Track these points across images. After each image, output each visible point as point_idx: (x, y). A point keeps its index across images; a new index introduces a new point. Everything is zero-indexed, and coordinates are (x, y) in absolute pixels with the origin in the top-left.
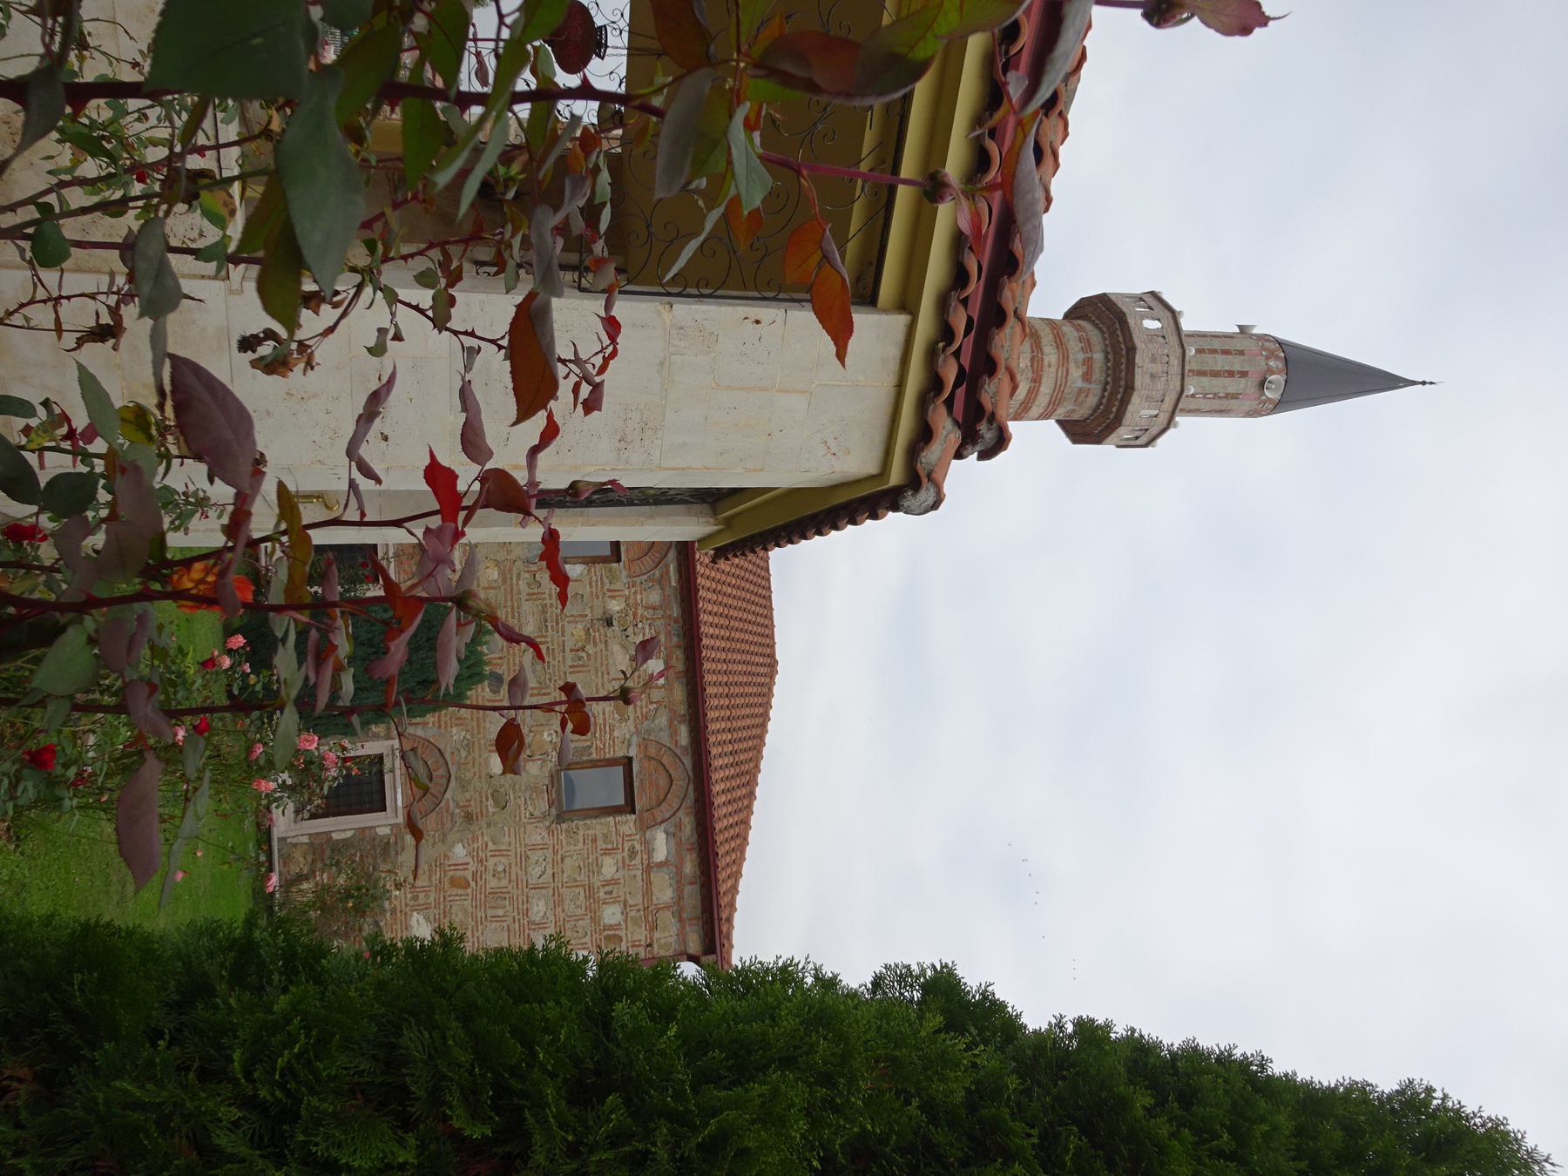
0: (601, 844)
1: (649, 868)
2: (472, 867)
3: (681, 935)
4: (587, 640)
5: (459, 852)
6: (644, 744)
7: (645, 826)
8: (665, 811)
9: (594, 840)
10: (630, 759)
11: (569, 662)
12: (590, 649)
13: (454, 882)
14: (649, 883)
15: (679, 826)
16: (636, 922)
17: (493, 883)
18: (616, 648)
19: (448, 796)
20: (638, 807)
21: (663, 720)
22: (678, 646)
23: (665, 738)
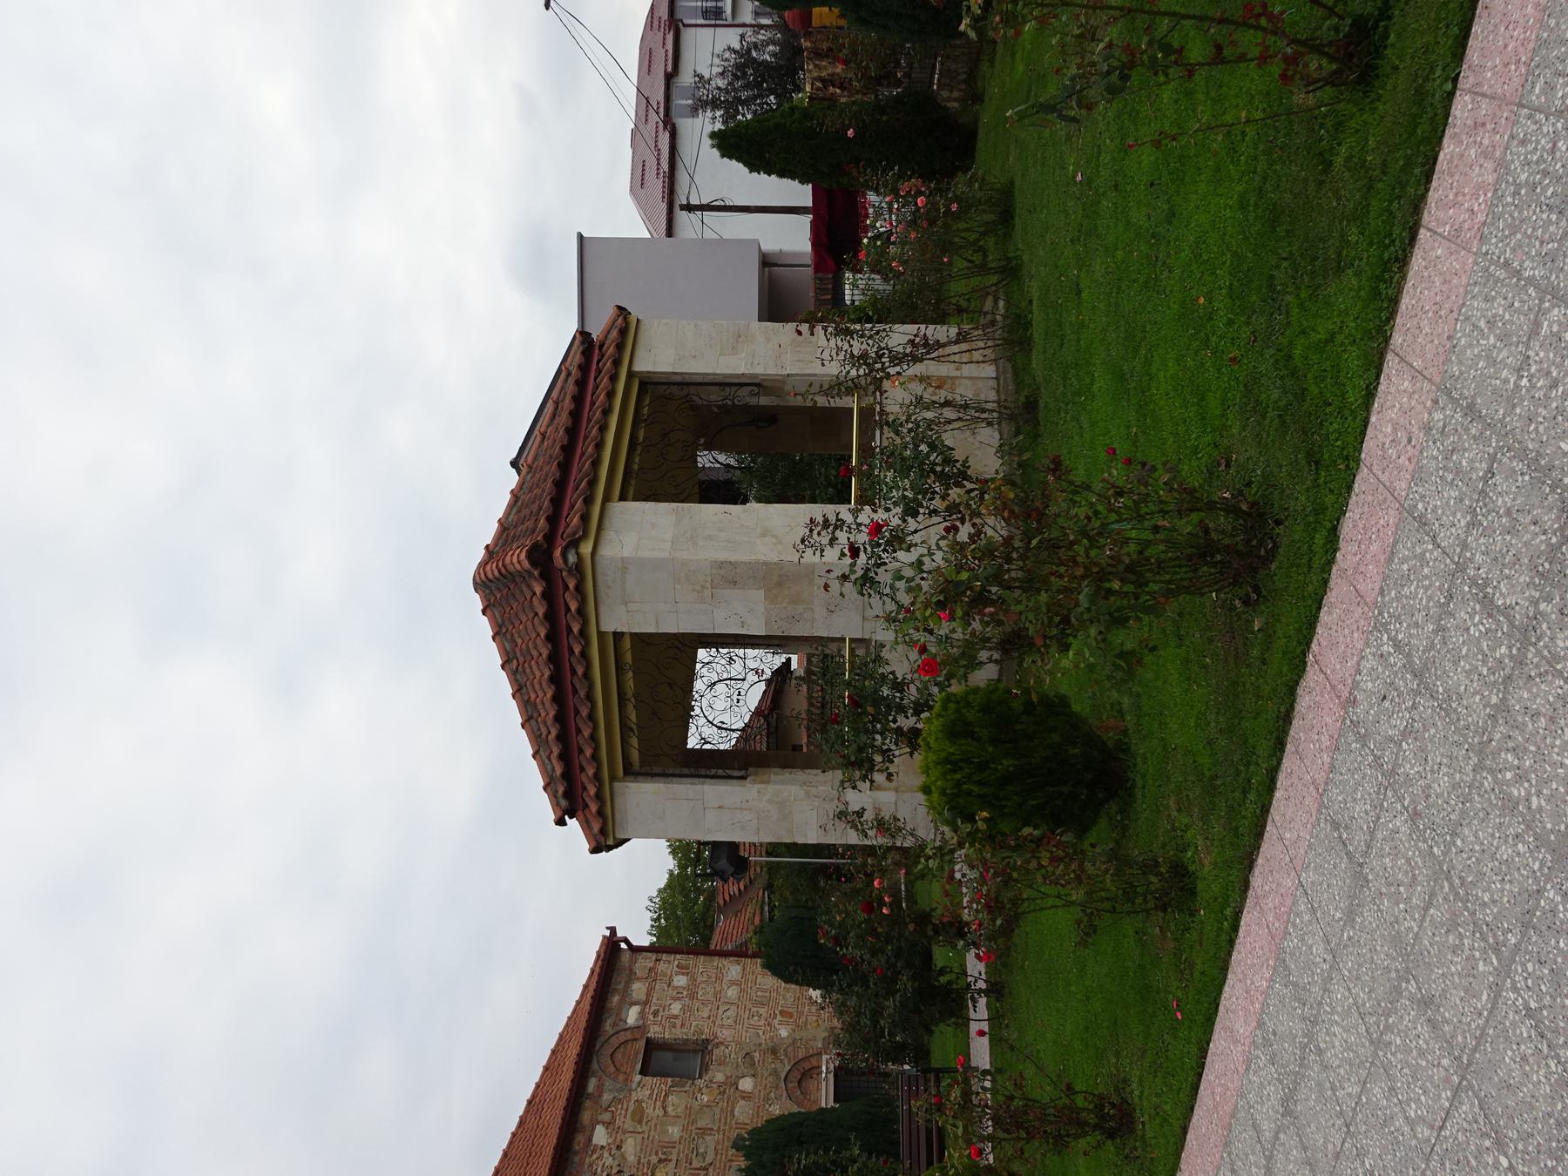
0: (679, 1022)
1: (646, 1003)
2: (776, 1022)
3: (633, 961)
4: (655, 1167)
5: (784, 1033)
6: (628, 1080)
7: (641, 1028)
8: (623, 1037)
9: (683, 1025)
10: (643, 1072)
11: (675, 1151)
12: (654, 1159)
13: (791, 1015)
14: (648, 994)
15: (615, 1024)
16: (665, 975)
17: (762, 1011)
18: (631, 1159)
19: (788, 1068)
20: (642, 1043)
21: (607, 1097)
22: (576, 1153)
23: (608, 1084)
